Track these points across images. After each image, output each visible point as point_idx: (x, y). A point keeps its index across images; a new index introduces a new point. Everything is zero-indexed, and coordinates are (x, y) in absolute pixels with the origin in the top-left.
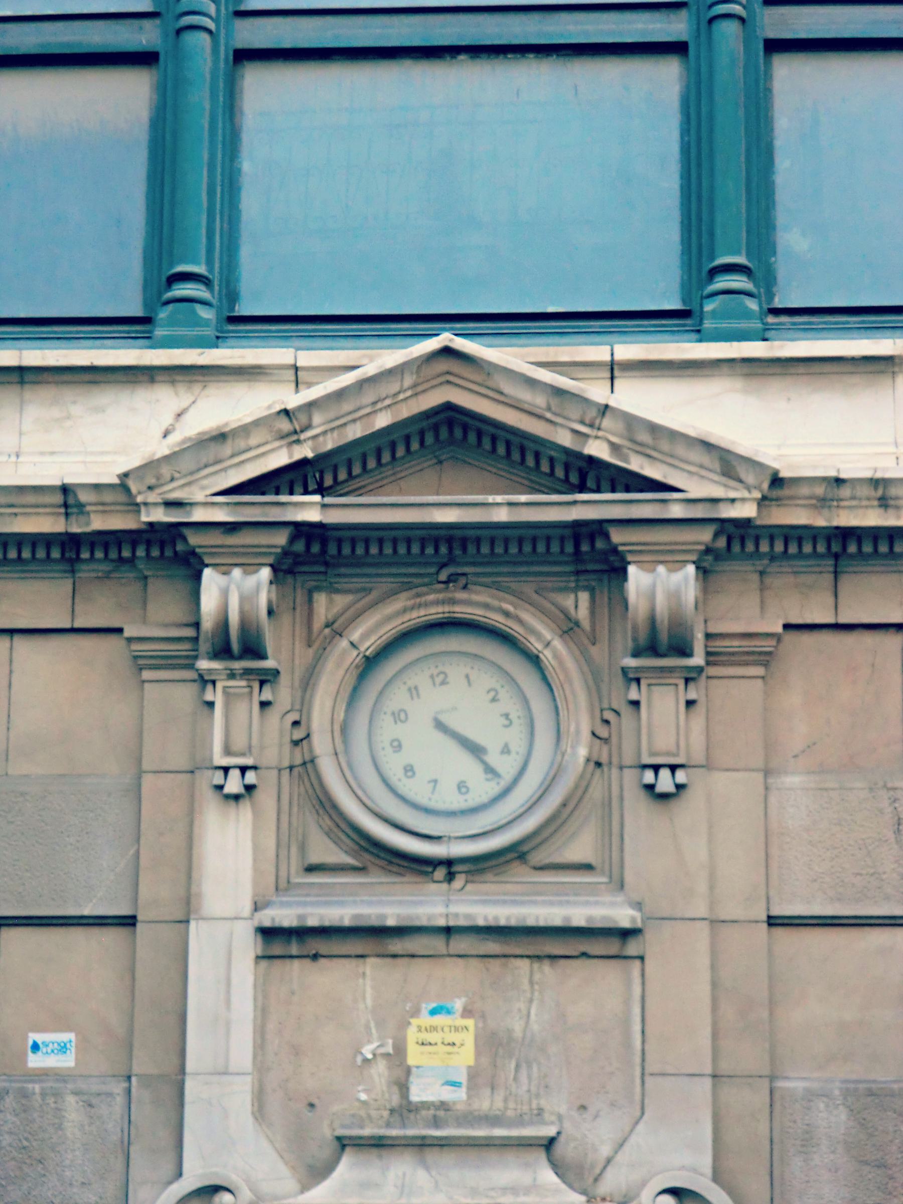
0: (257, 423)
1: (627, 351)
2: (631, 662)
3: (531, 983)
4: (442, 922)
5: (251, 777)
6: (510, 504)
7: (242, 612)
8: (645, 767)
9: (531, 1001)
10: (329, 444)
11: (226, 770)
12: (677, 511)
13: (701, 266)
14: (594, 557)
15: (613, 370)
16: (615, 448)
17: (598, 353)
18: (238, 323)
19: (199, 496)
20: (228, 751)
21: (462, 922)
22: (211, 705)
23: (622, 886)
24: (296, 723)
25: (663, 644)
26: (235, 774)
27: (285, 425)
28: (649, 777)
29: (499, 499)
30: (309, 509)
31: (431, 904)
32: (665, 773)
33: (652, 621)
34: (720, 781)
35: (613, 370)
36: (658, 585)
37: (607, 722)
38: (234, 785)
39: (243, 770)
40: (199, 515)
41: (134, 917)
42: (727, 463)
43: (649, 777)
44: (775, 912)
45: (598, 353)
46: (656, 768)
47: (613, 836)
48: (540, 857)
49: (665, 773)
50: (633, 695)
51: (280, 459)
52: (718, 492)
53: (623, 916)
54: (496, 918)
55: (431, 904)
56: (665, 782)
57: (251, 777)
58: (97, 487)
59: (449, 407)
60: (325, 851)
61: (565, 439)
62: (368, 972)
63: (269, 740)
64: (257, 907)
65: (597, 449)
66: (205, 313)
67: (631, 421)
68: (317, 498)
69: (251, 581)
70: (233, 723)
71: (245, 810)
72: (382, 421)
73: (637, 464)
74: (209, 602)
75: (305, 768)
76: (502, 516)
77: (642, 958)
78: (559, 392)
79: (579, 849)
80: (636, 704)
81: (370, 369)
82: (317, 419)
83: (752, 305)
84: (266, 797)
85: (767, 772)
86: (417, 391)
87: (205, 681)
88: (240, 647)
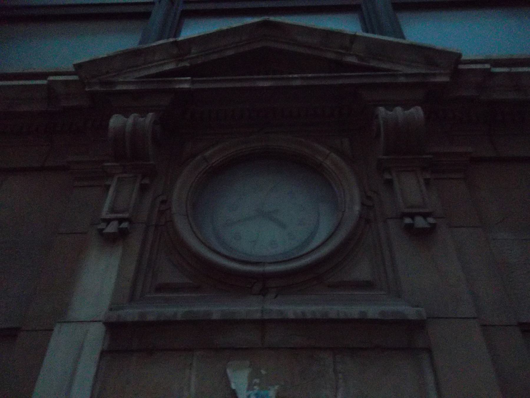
2: (385, 157)
3: (335, 371)
4: (258, 316)
5: (125, 225)
6: (302, 78)
8: (404, 215)
9: (337, 388)
11: (108, 221)
12: (402, 80)
20: (112, 210)
21: (274, 316)
22: (108, 187)
24: (163, 202)
26: (115, 223)
27: (175, 51)
28: (408, 220)
29: (296, 76)
31: (249, 307)
37: (369, 198)
38: (112, 228)
39: (121, 221)
41: (18, 329)
43: (408, 220)
46: (412, 216)
50: (387, 176)
51: (170, 66)
53: (410, 312)
54: (303, 313)
55: (249, 307)
56: (420, 222)
57: (125, 225)
62: (194, 365)
68: (189, 78)
71: (119, 251)
73: (374, 63)
77: (429, 350)
79: (362, 271)
80: (389, 183)
82: (194, 50)
84: (135, 242)
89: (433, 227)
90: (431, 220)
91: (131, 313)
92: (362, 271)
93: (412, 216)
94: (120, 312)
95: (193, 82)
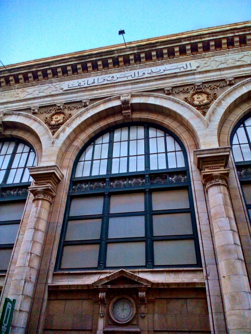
0: (105, 278)
1: (140, 270)
5: (103, 315)
7: (103, 298)
10: (111, 280)
11: (101, 314)
12: (143, 286)
13: (147, 262)
14: (136, 291)
15: (139, 272)
16: (137, 280)
17: (137, 270)
18: (106, 268)
19: (99, 285)
20: (101, 312)
22: (100, 307)
23: (139, 327)
25: (142, 300)
26: (102, 314)
28: (141, 315)
29: (127, 285)
30: (109, 286)
32: (143, 315)
33: (141, 297)
34: (149, 315)
35: (139, 272)
36: (142, 294)
38: (102, 316)
39: (103, 314)
40: (99, 287)
42: (148, 281)
43: (141, 315)
44: (154, 330)
45: (137, 270)
47: (138, 321)
48: (131, 324)
49: (143, 315)
51: (107, 282)
52: (147, 284)
53: (139, 330)
57: (103, 315)
58: (90, 285)
59: (122, 276)
60: (110, 323)
61: (133, 279)
63: (105, 310)
64: (104, 329)
65: (136, 280)
66: (102, 267)
67: (139, 278)
69: (104, 294)
70: (102, 309)
71: (103, 318)
72: (116, 277)
73: (139, 282)
74: (100, 296)
75: (108, 314)
76: (127, 287)
78: (132, 274)
80: (140, 307)
81: (115, 272)
82: (110, 277)
83: (152, 265)
84: (105, 317)
85: (154, 314)
86: (119, 274)
87: (100, 304)
88: (102, 301)
89: (144, 316)
90: (144, 315)
91: (106, 329)
92: (135, 323)
93: (142, 314)
94: (105, 329)
95: (111, 286)
